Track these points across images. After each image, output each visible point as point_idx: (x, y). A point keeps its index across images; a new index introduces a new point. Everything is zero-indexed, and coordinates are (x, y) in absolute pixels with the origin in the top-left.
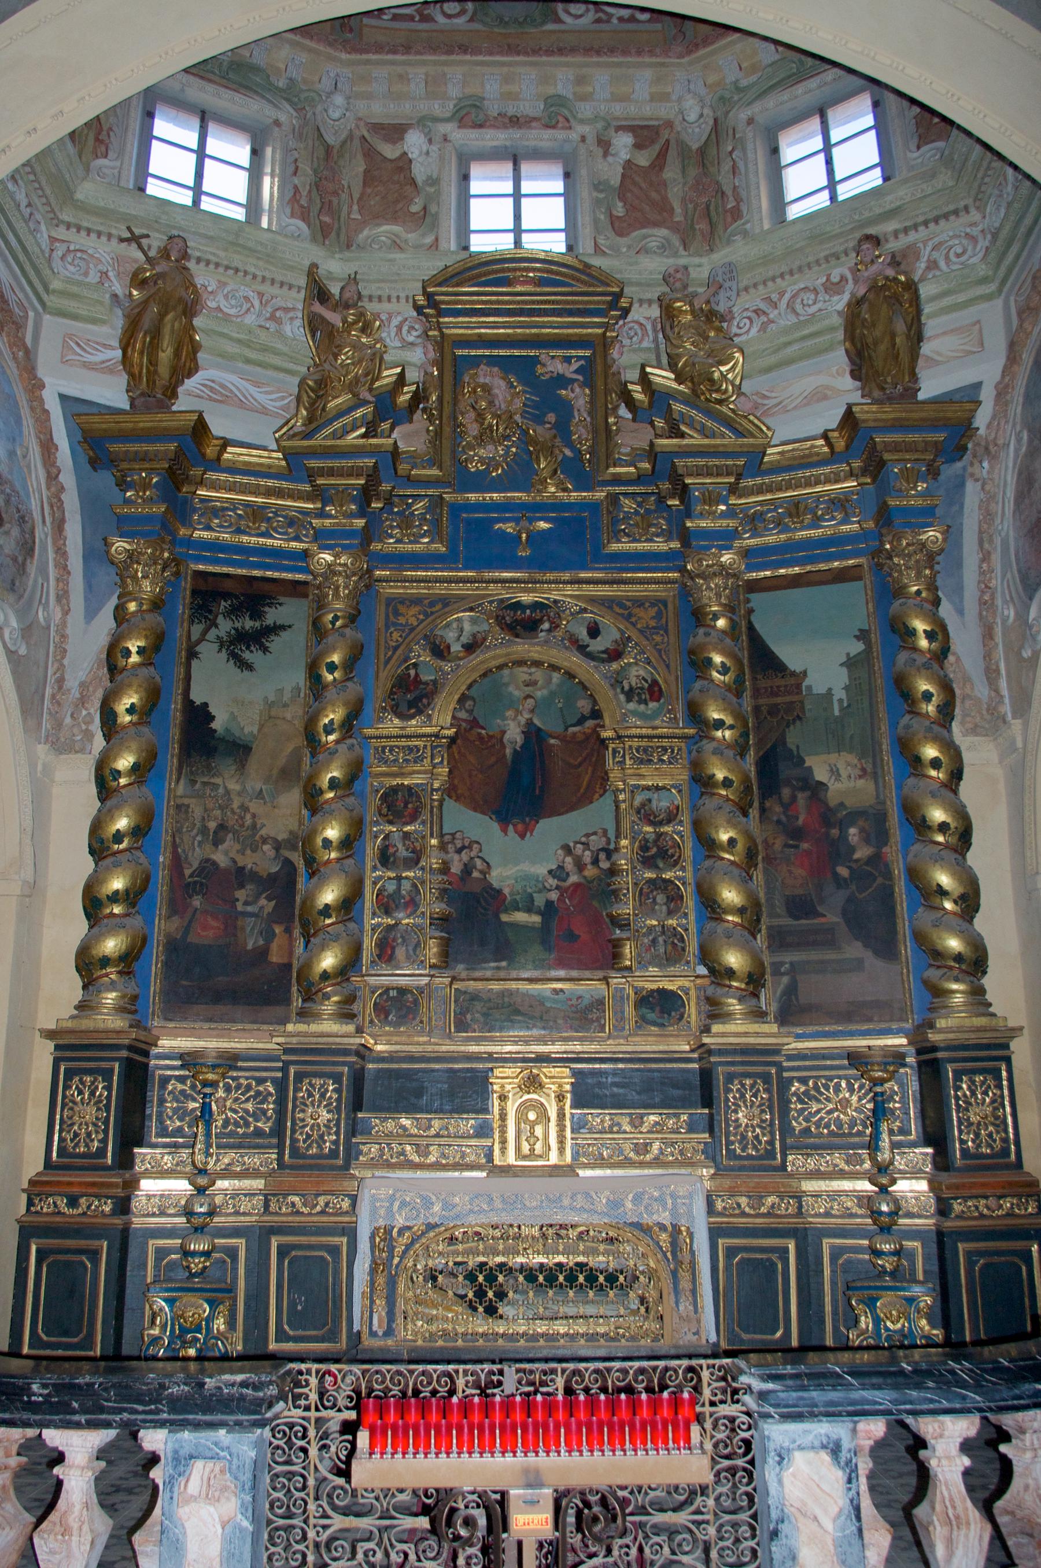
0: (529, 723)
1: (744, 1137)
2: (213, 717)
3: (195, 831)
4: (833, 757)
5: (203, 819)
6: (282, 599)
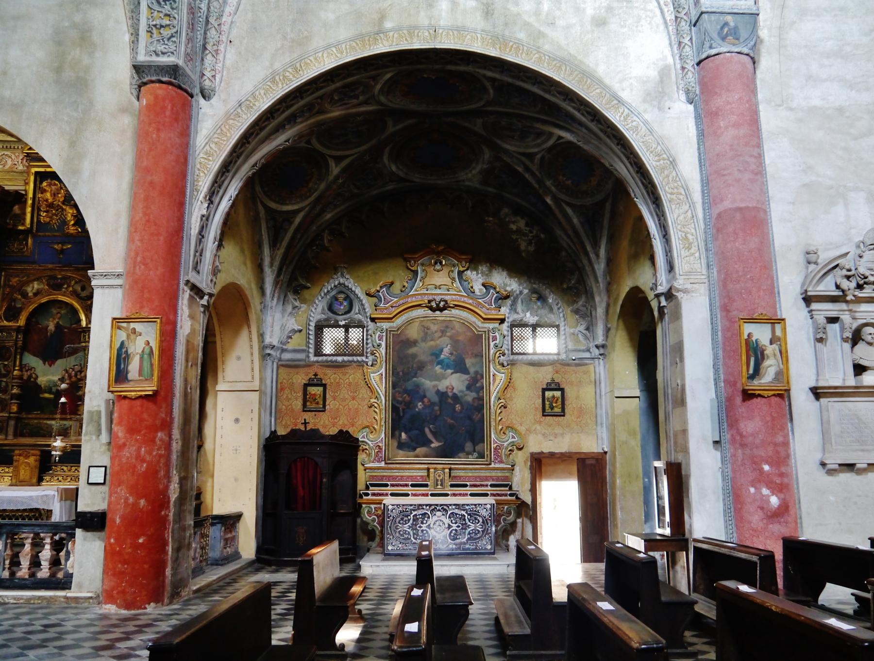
0: (58, 323)
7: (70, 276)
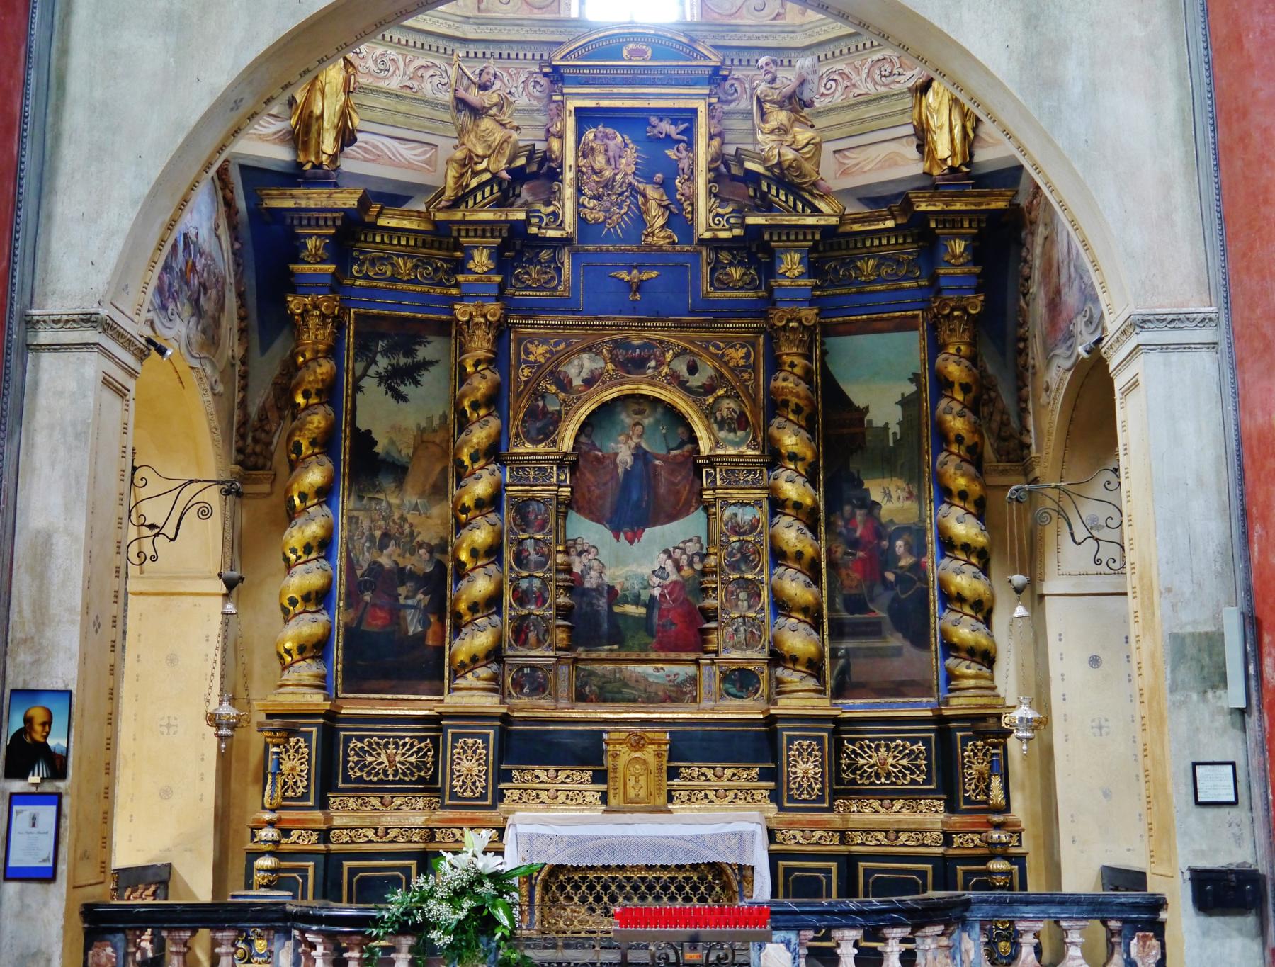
0: (638, 447)
1: (800, 786)
2: (375, 443)
3: (364, 539)
4: (886, 482)
5: (370, 528)
6: (430, 338)
7: (661, 342)
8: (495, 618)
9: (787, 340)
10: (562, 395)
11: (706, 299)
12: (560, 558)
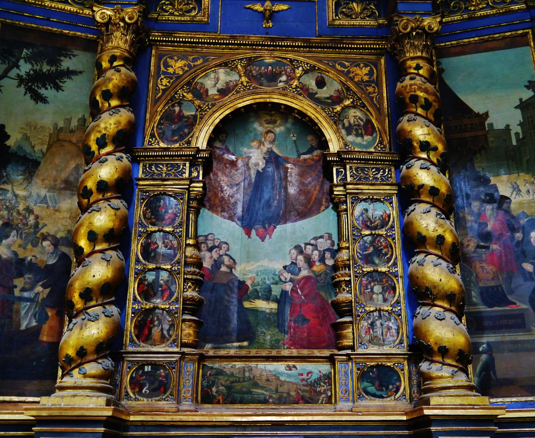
0: (270, 152)
2: (8, 137)
6: (76, 52)
7: (291, 61)
8: (114, 310)
9: (412, 45)
10: (197, 102)
11: (332, 26)
12: (190, 251)
